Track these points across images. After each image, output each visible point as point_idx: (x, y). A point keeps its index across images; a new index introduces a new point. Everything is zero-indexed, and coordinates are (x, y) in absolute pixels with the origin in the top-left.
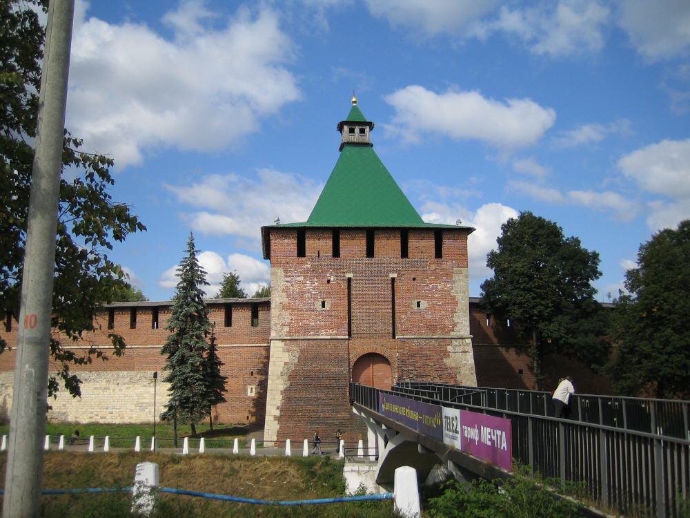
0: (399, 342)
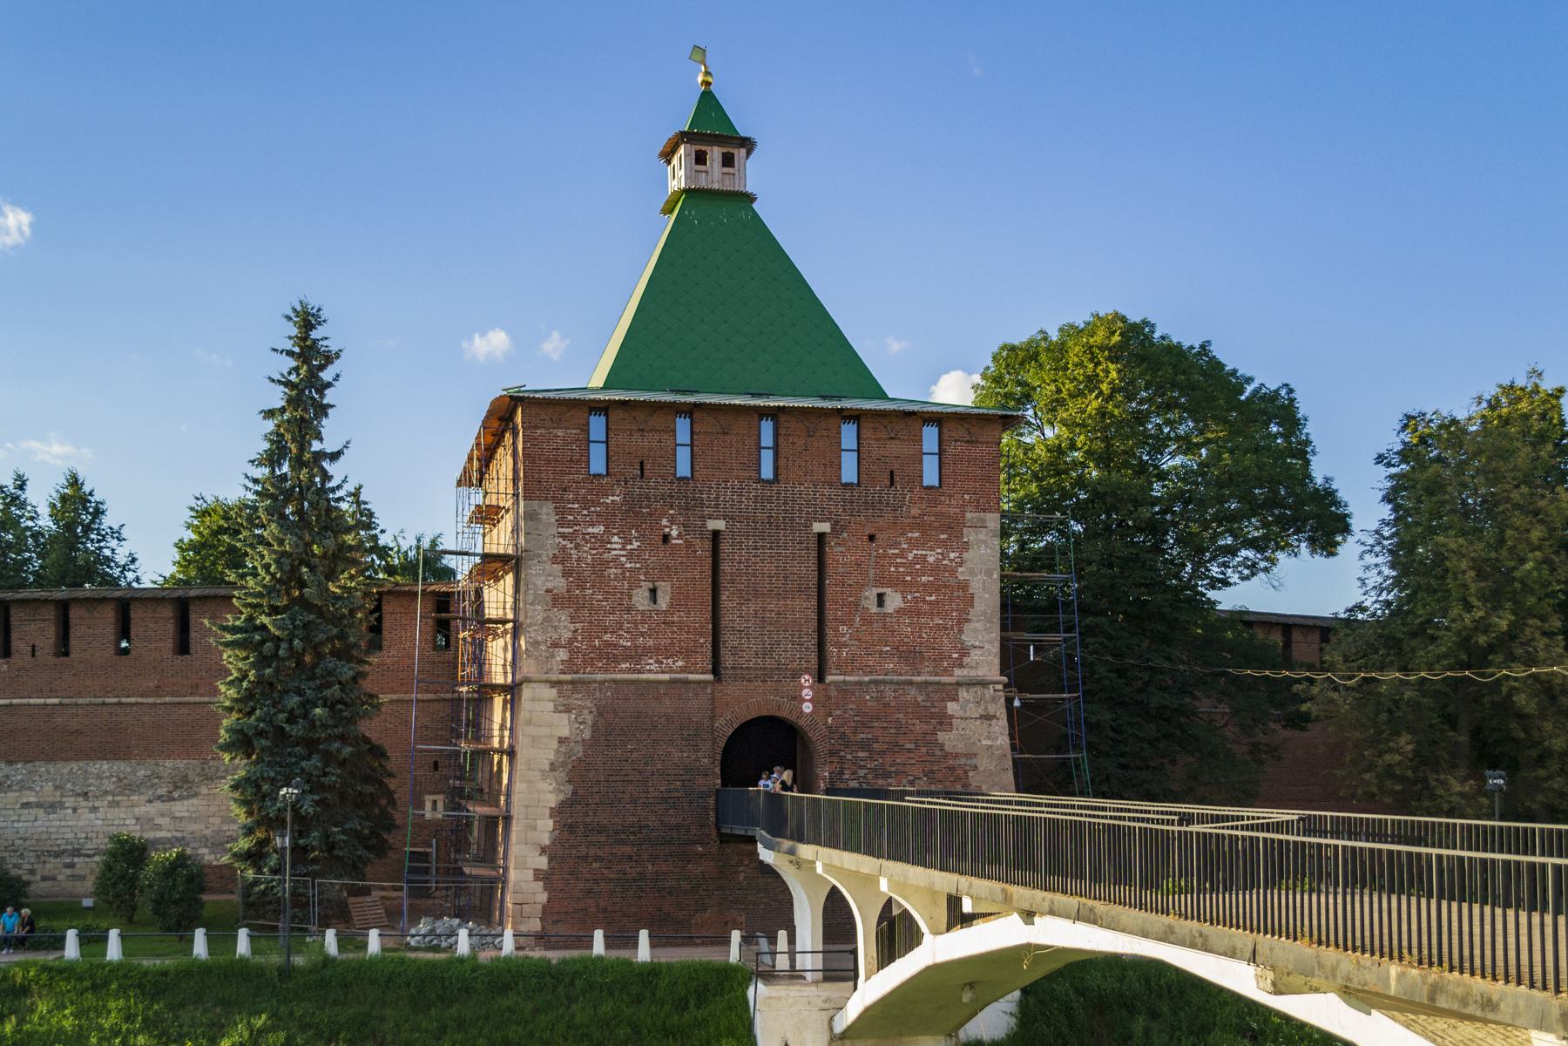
0: (834, 693)
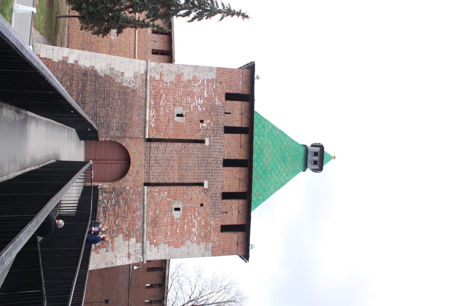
0: (140, 189)
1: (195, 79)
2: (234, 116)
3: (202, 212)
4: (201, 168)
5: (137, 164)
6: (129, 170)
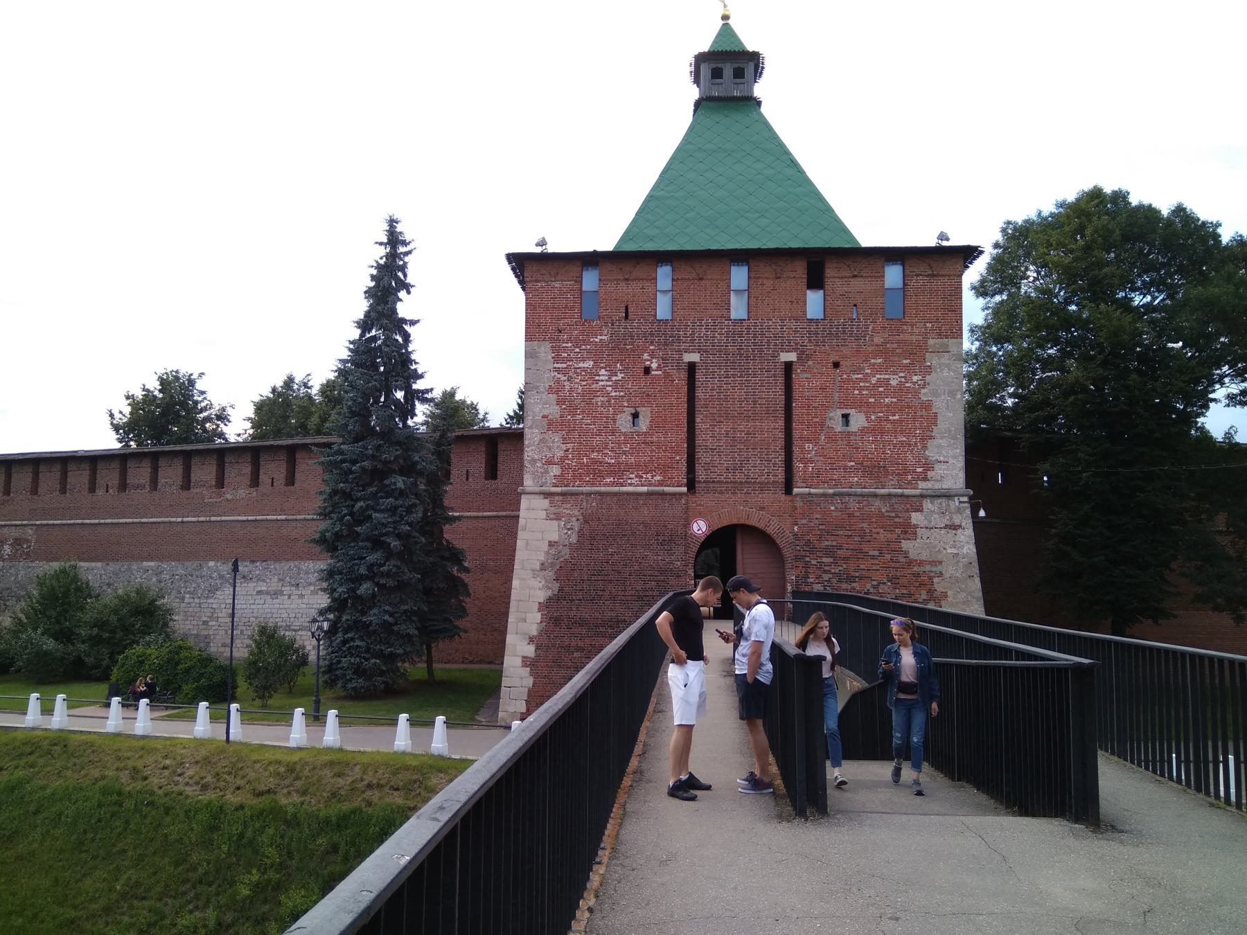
0: (799, 504)
1: (556, 389)
2: (633, 296)
3: (853, 363)
4: (751, 369)
5: (743, 510)
6: (758, 526)
